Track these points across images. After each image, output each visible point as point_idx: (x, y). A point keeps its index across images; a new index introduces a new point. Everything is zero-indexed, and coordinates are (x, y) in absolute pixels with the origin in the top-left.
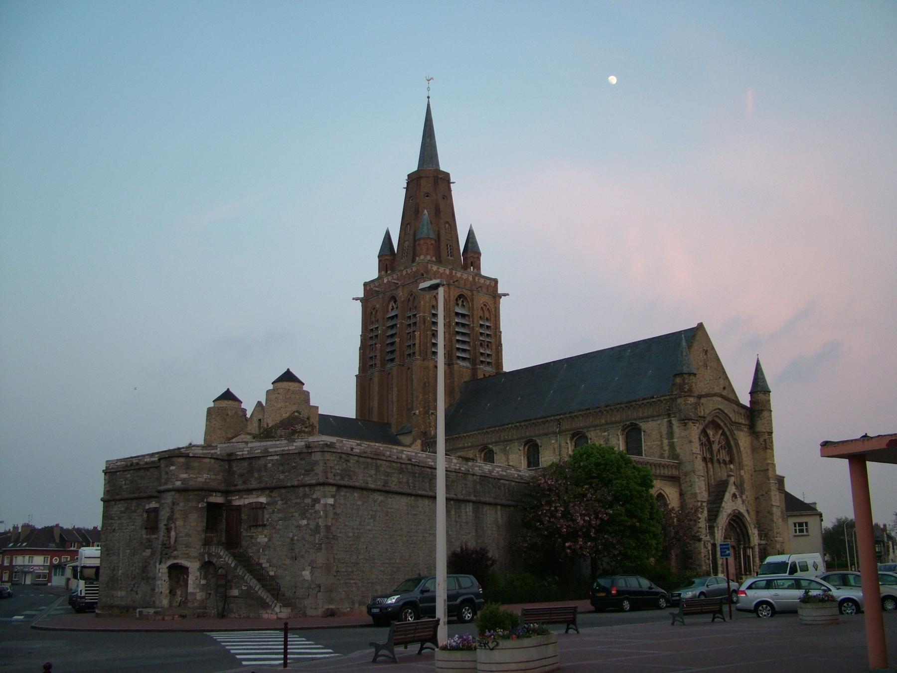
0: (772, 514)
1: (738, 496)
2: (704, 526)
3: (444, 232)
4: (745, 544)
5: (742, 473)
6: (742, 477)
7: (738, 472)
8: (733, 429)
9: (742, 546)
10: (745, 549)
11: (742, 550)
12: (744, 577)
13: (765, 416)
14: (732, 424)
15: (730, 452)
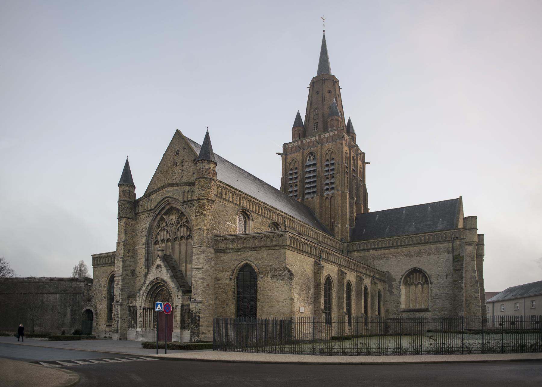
1: (163, 266)
2: (119, 294)
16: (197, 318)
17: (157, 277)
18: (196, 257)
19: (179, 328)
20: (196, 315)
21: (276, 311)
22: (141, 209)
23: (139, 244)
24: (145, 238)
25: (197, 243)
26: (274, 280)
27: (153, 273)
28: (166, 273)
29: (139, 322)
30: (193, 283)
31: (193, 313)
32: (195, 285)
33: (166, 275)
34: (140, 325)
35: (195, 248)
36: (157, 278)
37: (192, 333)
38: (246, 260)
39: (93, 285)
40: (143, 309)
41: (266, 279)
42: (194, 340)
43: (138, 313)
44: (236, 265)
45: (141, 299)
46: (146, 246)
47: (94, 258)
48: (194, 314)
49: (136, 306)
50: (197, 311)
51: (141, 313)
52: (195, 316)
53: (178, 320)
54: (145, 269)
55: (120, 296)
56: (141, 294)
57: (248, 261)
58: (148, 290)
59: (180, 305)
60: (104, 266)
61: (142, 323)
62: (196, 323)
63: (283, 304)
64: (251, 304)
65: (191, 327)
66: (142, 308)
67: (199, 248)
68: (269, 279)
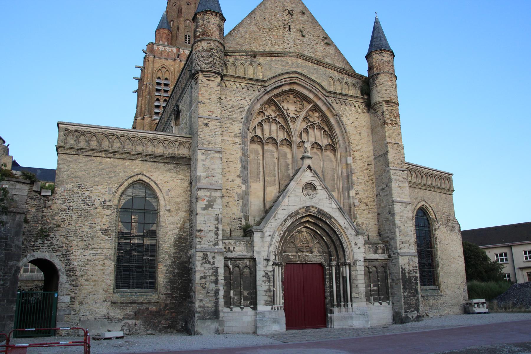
0: (393, 215)
1: (319, 188)
2: (213, 228)
3: (183, 26)
4: (338, 258)
5: (350, 160)
6: (347, 165)
7: (344, 160)
8: (330, 102)
9: (334, 263)
10: (338, 266)
11: (334, 268)
12: (336, 309)
13: (381, 81)
14: (328, 95)
15: (330, 133)
16: (413, 280)
17: (308, 204)
18: (397, 184)
19: (364, 299)
20: (411, 275)
21: (454, 271)
22: (231, 70)
23: (224, 133)
24: (241, 125)
25: (394, 163)
26: (449, 232)
27: (297, 196)
28: (328, 201)
29: (264, 293)
30: (399, 225)
31: (405, 273)
32: (402, 228)
33: (328, 205)
34: (268, 299)
35: (395, 171)
36: (307, 207)
37: (406, 306)
38: (423, 201)
39: (57, 196)
40: (273, 265)
41: (442, 229)
42: (412, 317)
43: (260, 274)
44: (414, 206)
45: (267, 244)
46: (242, 140)
47: (67, 130)
48: (407, 275)
49: (254, 260)
50: (411, 268)
51: (269, 273)
52: (410, 277)
53: (360, 286)
54: (243, 183)
55: (217, 234)
56: (267, 234)
57: (425, 203)
58: (285, 228)
59: (362, 259)
60: (103, 155)
61: (272, 294)
62: (411, 288)
63: (459, 262)
64: (429, 261)
65: (404, 296)
66: (271, 263)
67: (401, 171)
68: (445, 230)
